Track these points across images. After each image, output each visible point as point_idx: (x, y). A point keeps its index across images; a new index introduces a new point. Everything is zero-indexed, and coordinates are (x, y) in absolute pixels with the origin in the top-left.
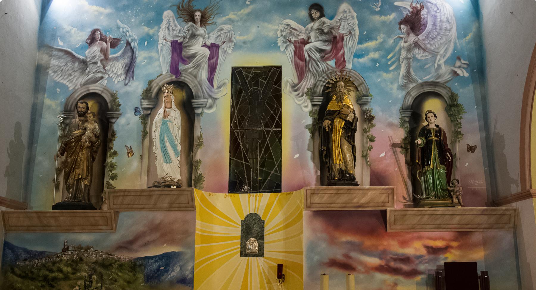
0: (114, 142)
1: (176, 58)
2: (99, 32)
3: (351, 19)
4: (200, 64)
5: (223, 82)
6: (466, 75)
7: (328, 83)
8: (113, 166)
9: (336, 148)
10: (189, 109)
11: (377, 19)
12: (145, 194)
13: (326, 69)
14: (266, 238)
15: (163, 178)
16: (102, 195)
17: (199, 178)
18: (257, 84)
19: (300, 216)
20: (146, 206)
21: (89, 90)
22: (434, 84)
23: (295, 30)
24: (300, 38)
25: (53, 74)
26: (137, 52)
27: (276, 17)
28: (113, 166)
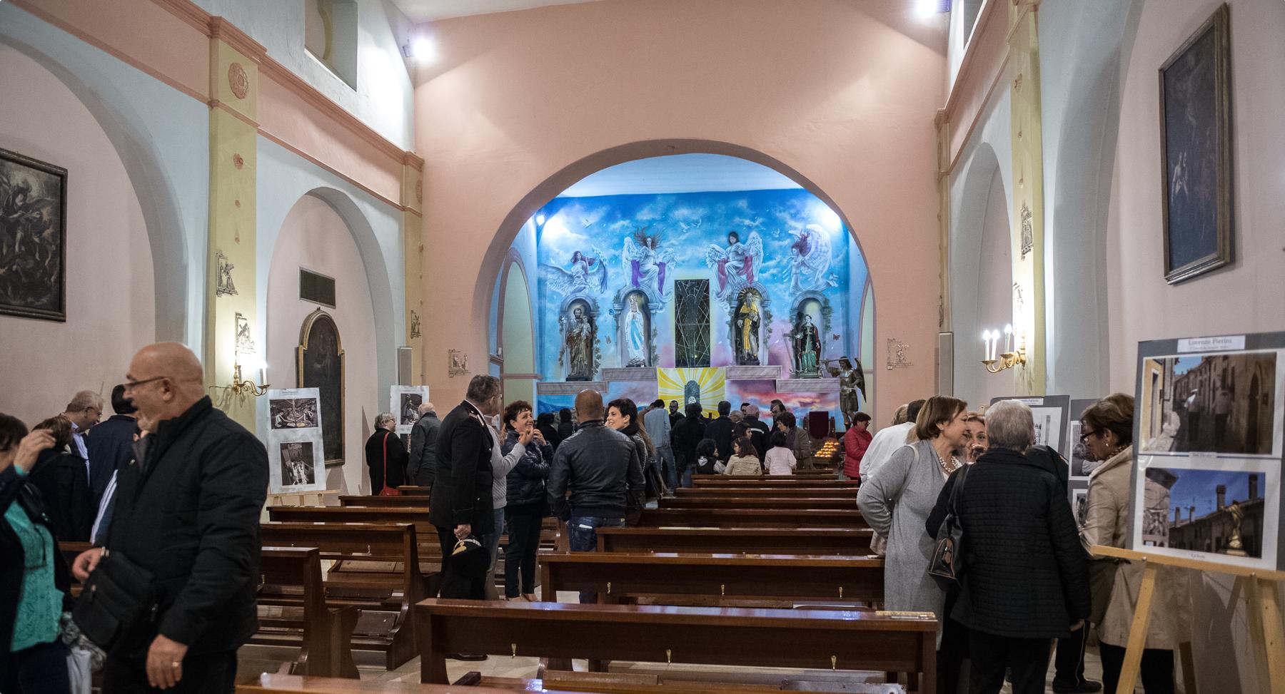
8: (598, 350)
9: (746, 339)
10: (646, 310)
11: (776, 244)
17: (656, 358)
22: (814, 292)
28: (598, 350)
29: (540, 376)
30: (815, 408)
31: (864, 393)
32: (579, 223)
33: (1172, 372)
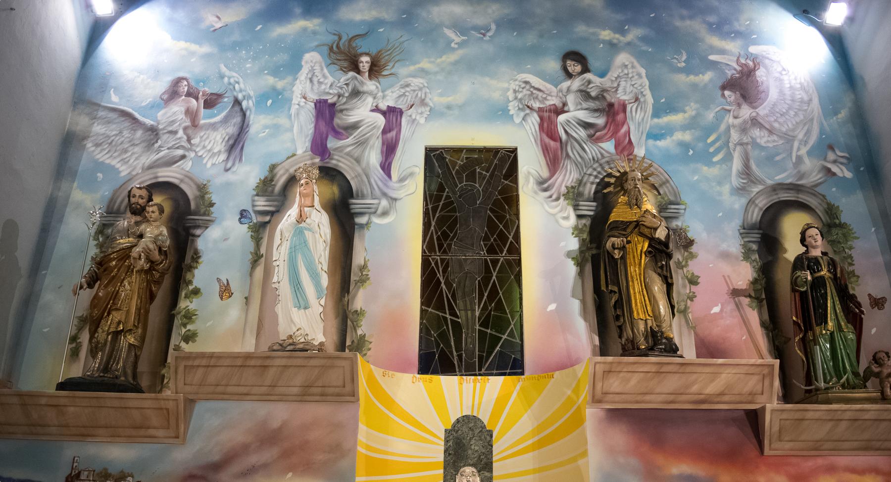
0: (196, 272)
1: (323, 127)
2: (186, 83)
3: (636, 77)
4: (367, 140)
5: (409, 171)
6: (848, 175)
7: (610, 175)
8: (189, 317)
10: (345, 216)
11: (682, 79)
12: (253, 362)
13: (599, 156)
14: (495, 465)
15: (291, 337)
16: (164, 371)
18: (472, 177)
20: (256, 390)
21: (157, 177)
22: (795, 188)
23: (539, 90)
24: (548, 103)
25: (93, 148)
26: (252, 117)
28: (189, 317)
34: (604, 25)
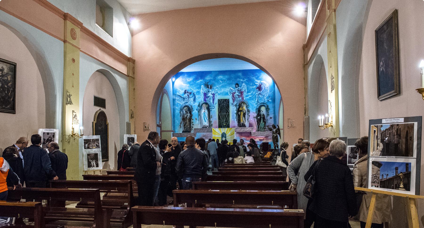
8: (193, 122)
9: (241, 118)
10: (209, 109)
11: (251, 87)
17: (212, 125)
19: (234, 133)
22: (264, 103)
27: (228, 87)
28: (193, 122)
29: (174, 131)
30: (264, 141)
31: (280, 136)
32: (186, 81)
33: (380, 130)
34: (241, 79)
